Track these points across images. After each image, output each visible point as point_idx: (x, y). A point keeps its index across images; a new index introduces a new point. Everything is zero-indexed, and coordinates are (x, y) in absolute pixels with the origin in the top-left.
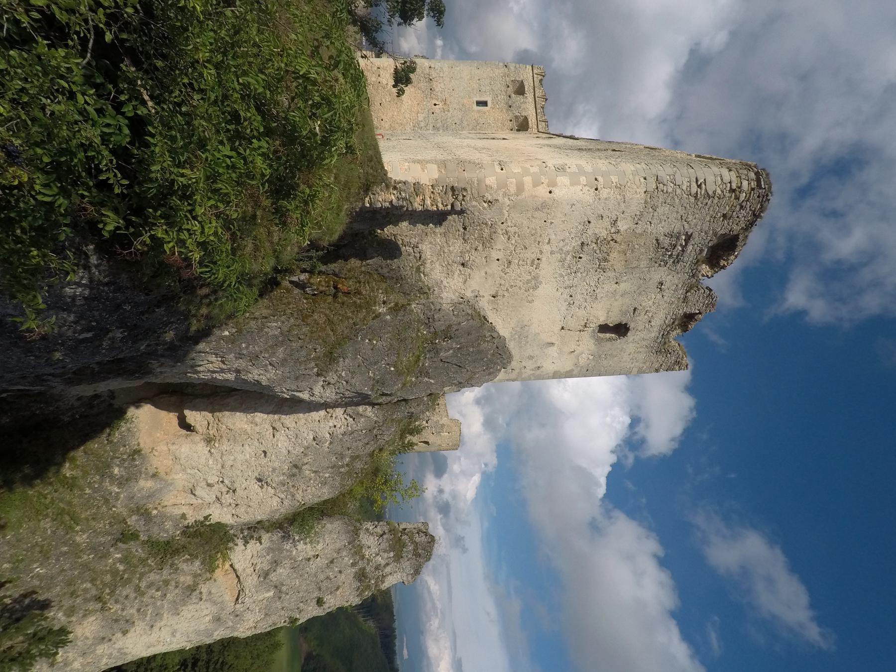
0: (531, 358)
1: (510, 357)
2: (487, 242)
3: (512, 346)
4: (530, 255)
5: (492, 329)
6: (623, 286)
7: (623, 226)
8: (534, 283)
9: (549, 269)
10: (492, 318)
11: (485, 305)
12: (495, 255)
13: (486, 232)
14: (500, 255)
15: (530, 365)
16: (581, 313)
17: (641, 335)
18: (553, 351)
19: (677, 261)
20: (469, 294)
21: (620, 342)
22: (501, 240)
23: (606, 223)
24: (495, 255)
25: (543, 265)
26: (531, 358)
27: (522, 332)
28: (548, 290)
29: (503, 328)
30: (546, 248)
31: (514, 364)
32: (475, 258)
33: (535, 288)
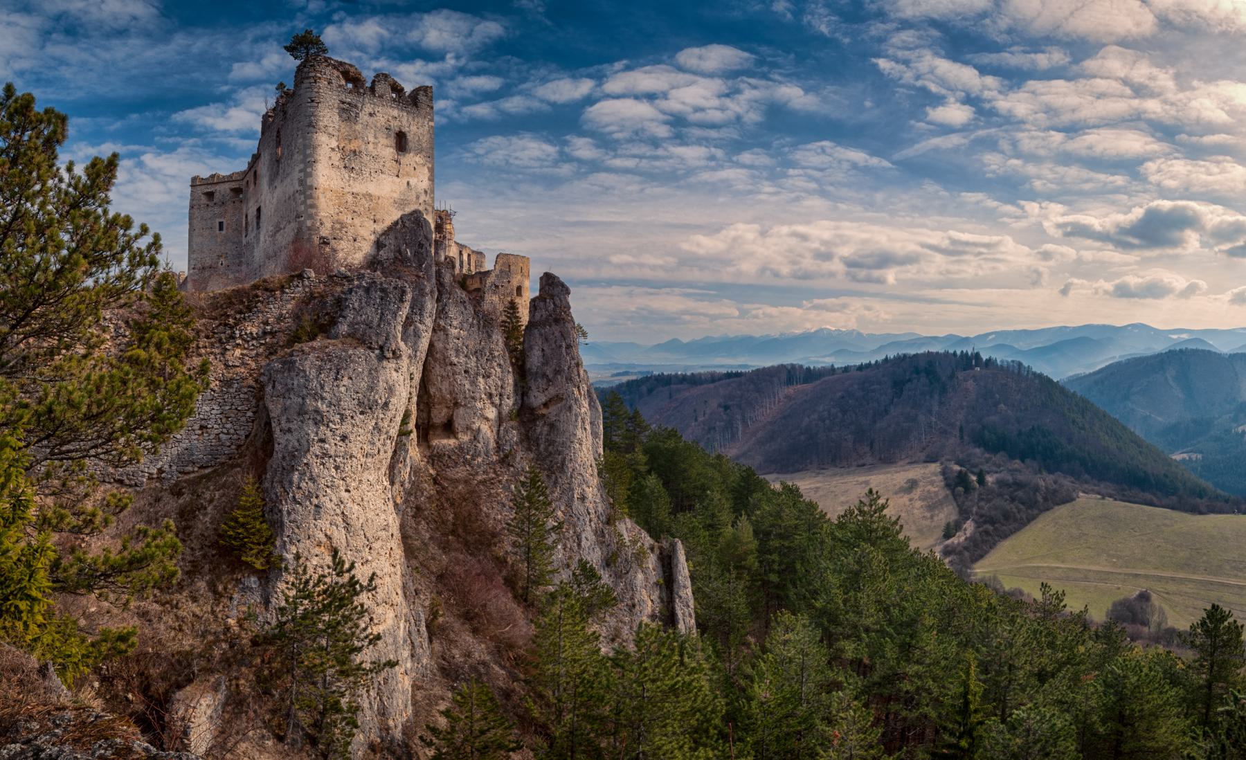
0: (418, 197)
1: (415, 212)
2: (343, 225)
3: (408, 210)
4: (350, 198)
5: (396, 223)
6: (371, 139)
7: (334, 144)
8: (369, 196)
9: (358, 187)
10: (388, 223)
11: (380, 228)
12: (350, 221)
13: (338, 226)
14: (350, 217)
15: (423, 198)
16: (388, 164)
17: (405, 122)
18: (413, 181)
19: (356, 106)
20: (373, 237)
21: (410, 137)
22: (343, 217)
23: (333, 154)
24: (350, 221)
25: (355, 190)
26: (418, 197)
27: (401, 203)
28: (371, 188)
29: (396, 215)
30: (347, 190)
31: (421, 208)
32: (351, 231)
33: (370, 195)
